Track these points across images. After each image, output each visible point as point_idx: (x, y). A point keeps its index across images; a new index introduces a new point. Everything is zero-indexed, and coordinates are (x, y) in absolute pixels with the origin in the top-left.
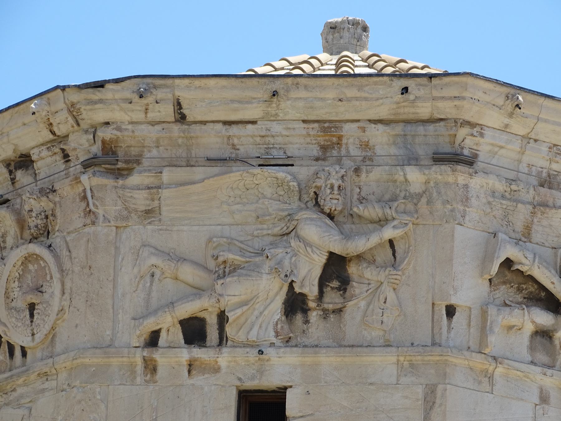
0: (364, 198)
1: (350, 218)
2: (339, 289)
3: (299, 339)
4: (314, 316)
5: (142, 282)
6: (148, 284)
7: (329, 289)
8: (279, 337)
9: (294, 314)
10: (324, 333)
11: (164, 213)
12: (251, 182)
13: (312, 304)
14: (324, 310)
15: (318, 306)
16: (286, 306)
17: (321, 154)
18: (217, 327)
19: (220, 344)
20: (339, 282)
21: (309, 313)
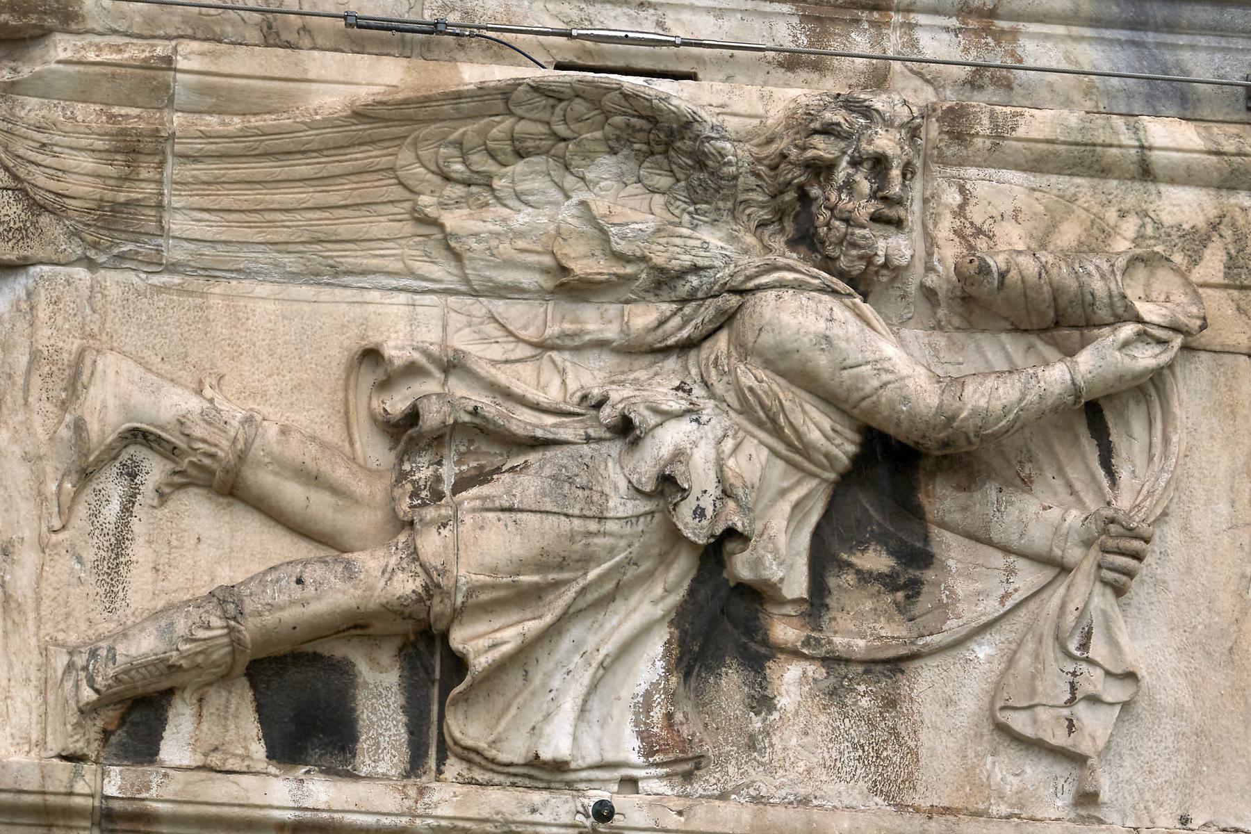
0: (979, 232)
1: (924, 307)
2: (889, 582)
3: (731, 770)
4: (791, 681)
5: (88, 495)
6: (115, 506)
7: (850, 578)
8: (658, 758)
9: (710, 669)
10: (834, 754)
11: (178, 224)
12: (542, 129)
13: (785, 631)
14: (832, 661)
15: (806, 643)
16: (684, 633)
17: (804, 40)
18: (401, 700)
19: (415, 765)
20: (891, 553)
21: (772, 668)
